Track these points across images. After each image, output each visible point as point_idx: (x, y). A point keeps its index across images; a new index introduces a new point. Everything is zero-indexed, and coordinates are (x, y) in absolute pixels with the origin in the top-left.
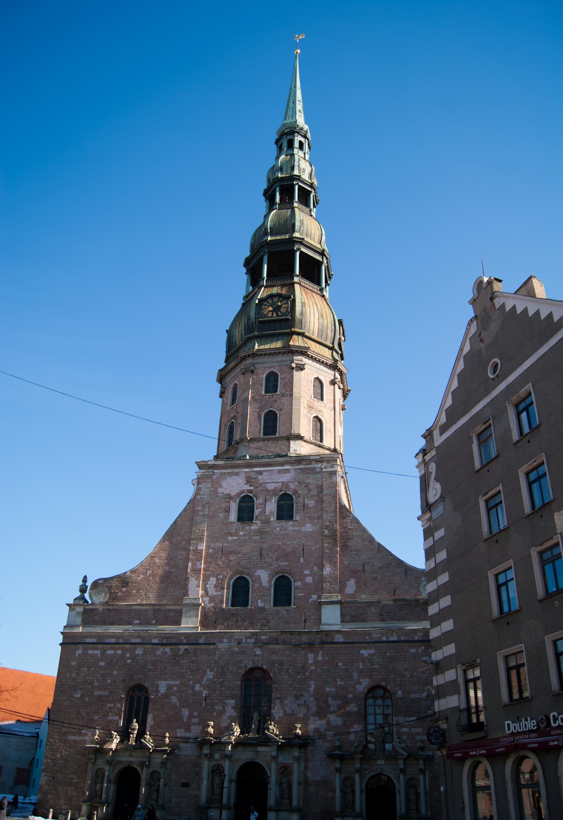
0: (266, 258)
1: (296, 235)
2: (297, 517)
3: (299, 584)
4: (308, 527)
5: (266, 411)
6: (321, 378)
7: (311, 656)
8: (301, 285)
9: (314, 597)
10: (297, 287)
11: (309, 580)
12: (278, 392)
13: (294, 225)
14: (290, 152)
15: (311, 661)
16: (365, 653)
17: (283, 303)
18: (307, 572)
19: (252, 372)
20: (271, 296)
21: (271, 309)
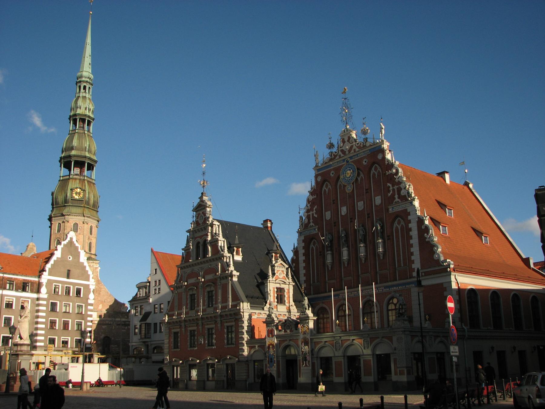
1: (87, 154)
8: (88, 181)
10: (86, 182)
13: (86, 147)
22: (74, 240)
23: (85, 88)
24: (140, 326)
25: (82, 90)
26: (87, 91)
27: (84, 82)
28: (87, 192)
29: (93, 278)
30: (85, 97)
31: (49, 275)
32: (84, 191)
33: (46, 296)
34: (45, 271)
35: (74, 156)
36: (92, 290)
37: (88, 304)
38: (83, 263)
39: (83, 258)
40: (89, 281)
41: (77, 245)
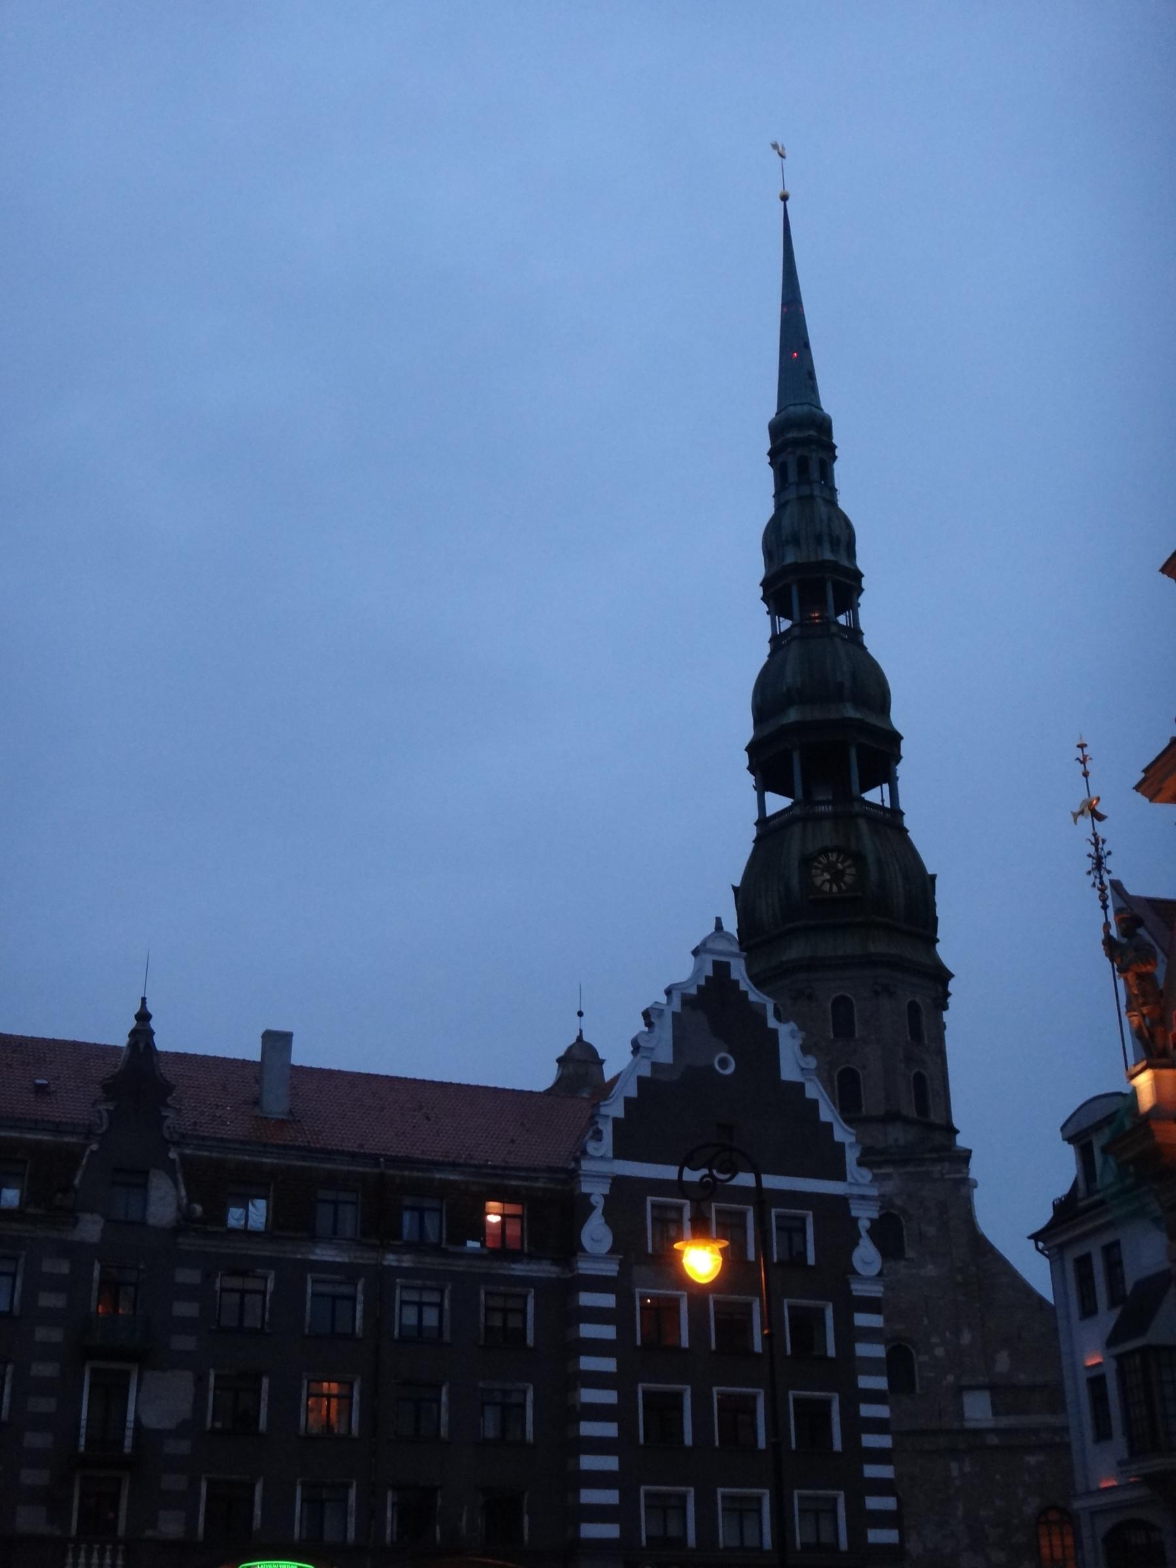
0: (796, 756)
1: (850, 712)
2: (910, 1253)
3: (924, 1358)
4: (930, 1270)
5: (840, 1069)
6: (917, 1000)
7: (954, 1466)
9: (950, 1378)
11: (940, 1352)
12: (857, 1035)
14: (805, 490)
15: (955, 1473)
16: (1032, 1460)
17: (846, 864)
18: (935, 1340)
19: (810, 997)
20: (825, 851)
21: (827, 876)
22: (738, 970)
23: (803, 465)
24: (1121, 1373)
25: (792, 476)
26: (816, 475)
27: (796, 443)
28: (871, 859)
29: (860, 1163)
30: (811, 497)
31: (621, 1152)
32: (858, 858)
33: (611, 1269)
34: (598, 1136)
35: (800, 727)
36: (864, 1225)
37: (849, 1305)
38: (800, 1087)
39: (792, 1062)
40: (840, 1176)
41: (754, 996)
